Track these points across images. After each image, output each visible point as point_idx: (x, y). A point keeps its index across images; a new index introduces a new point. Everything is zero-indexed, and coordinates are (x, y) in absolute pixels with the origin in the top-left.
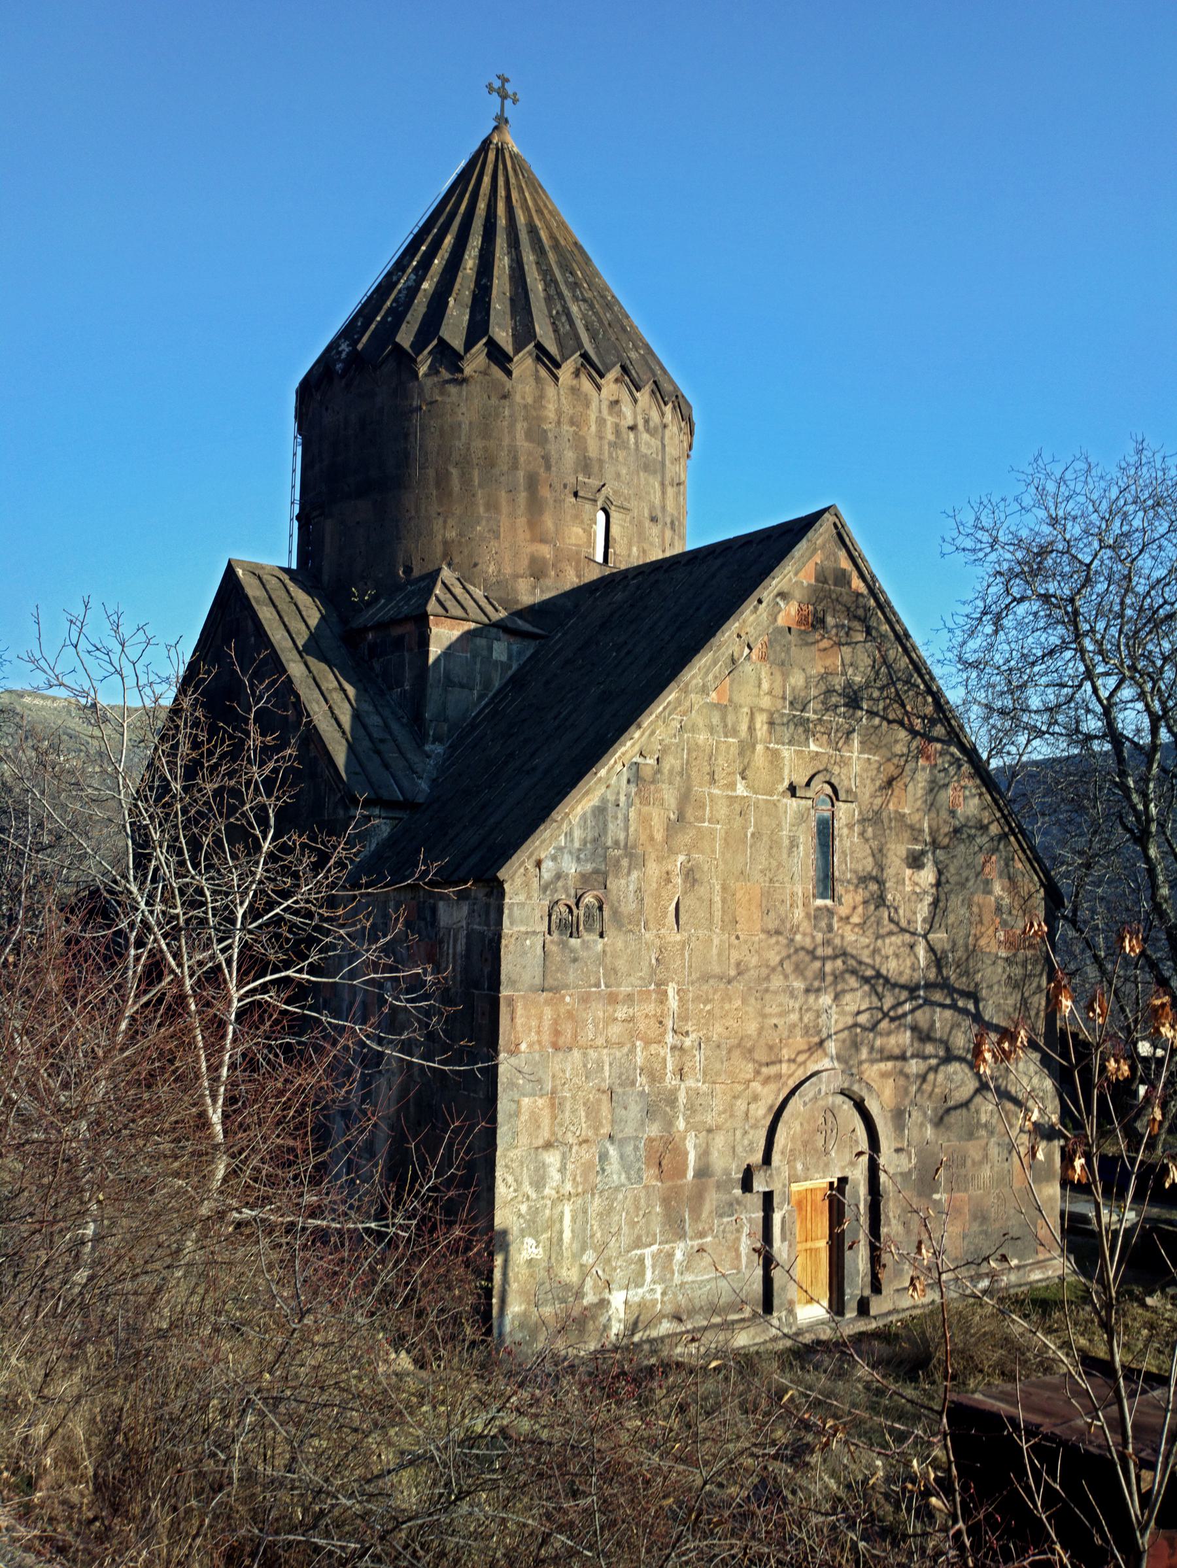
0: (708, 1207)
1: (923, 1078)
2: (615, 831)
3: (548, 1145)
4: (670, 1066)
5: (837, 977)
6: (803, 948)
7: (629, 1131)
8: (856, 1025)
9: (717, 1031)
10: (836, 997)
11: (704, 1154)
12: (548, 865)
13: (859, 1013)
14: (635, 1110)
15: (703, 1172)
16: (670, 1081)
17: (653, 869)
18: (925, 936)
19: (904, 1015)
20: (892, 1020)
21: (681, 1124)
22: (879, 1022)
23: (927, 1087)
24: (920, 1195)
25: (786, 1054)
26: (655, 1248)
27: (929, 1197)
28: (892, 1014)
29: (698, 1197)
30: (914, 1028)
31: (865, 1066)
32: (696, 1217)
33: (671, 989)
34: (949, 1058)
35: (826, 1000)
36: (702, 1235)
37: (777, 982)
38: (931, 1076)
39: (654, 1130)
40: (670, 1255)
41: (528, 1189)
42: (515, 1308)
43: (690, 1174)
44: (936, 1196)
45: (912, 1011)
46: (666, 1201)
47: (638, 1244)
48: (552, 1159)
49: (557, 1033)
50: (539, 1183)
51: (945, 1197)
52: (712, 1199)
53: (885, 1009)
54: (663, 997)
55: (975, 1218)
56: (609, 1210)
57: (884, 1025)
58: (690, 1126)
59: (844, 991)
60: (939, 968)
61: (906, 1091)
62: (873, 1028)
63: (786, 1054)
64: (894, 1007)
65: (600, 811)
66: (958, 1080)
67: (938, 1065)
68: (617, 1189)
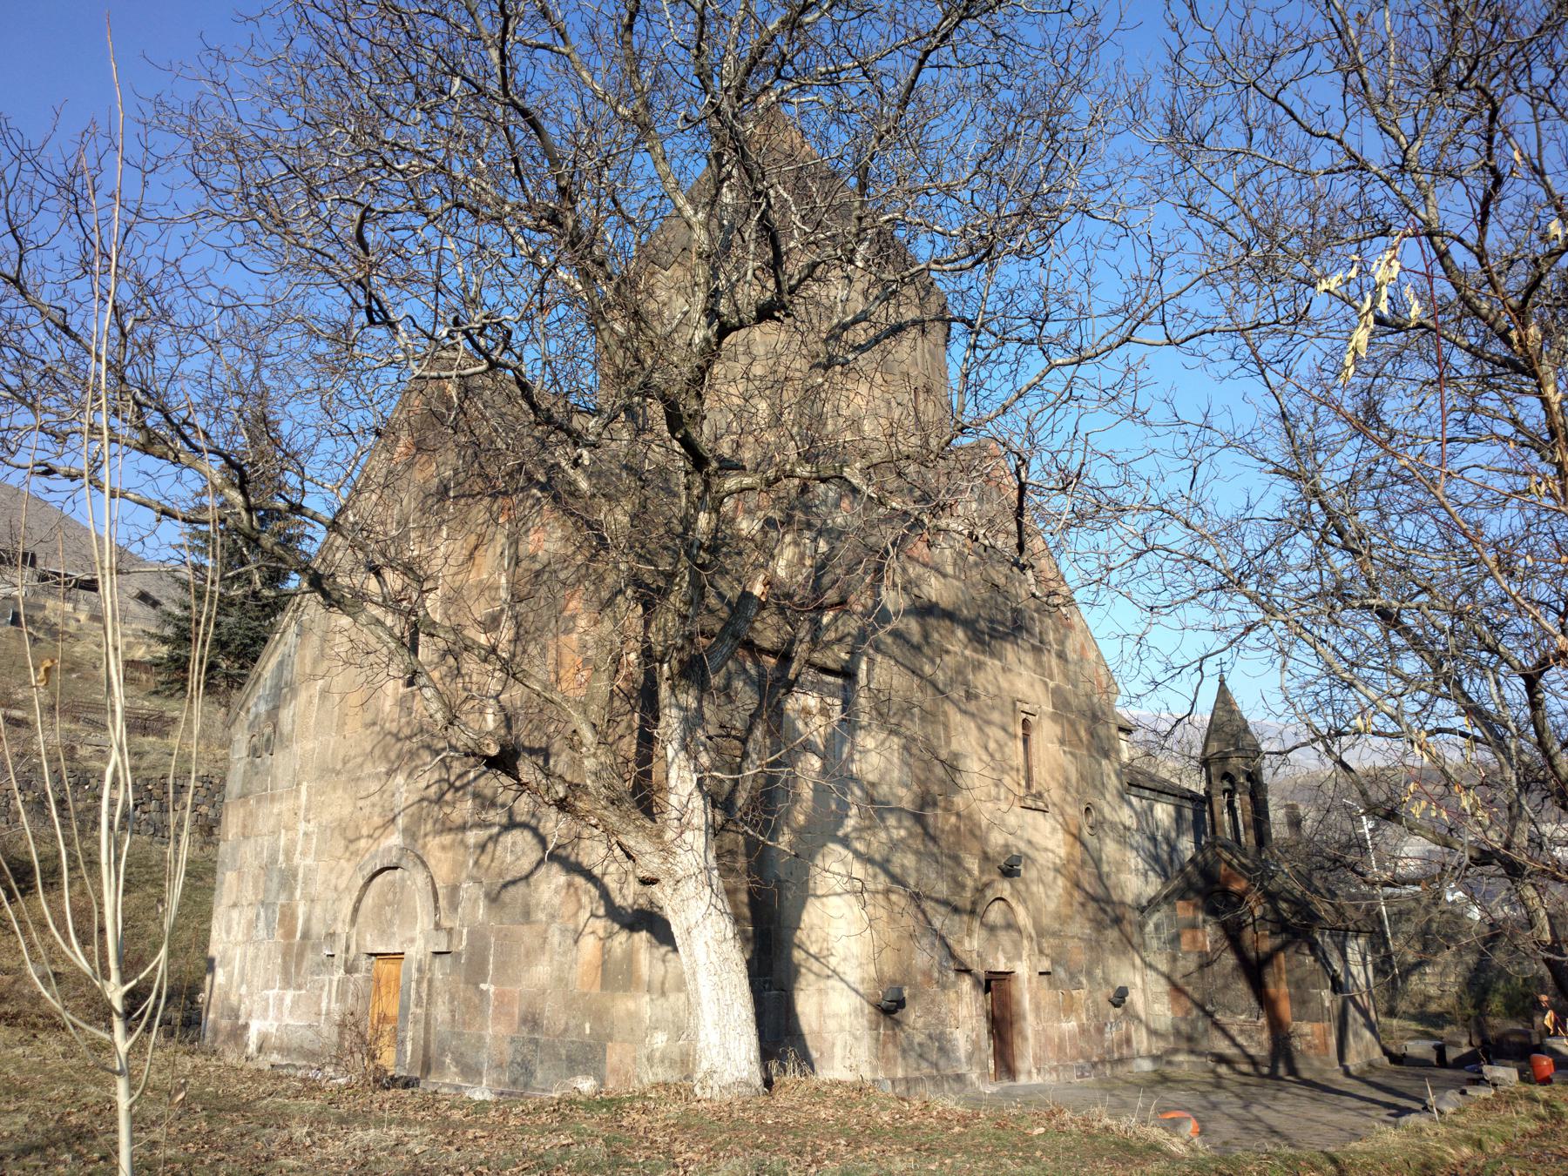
0: (306, 964)
1: (483, 847)
2: (287, 676)
3: (235, 905)
4: (299, 848)
5: (413, 754)
6: (390, 733)
7: (271, 899)
8: (422, 800)
9: (326, 817)
10: (410, 775)
11: (308, 920)
12: (253, 710)
13: (428, 787)
14: (274, 885)
15: (306, 935)
16: (297, 859)
17: (303, 696)
18: (496, 698)
19: (469, 783)
20: (457, 790)
21: (298, 894)
22: (443, 794)
23: (485, 860)
24: (467, 982)
25: (365, 831)
26: (276, 991)
27: (476, 985)
28: (458, 784)
29: (301, 955)
30: (476, 795)
31: (429, 838)
32: (298, 973)
33: (303, 788)
34: (511, 825)
35: (400, 779)
36: (299, 987)
37: (368, 768)
38: (490, 846)
39: (282, 900)
40: (282, 1000)
41: (224, 935)
42: (211, 1016)
43: (298, 935)
44: (483, 986)
45: (475, 779)
46: (284, 955)
47: (267, 986)
48: (235, 914)
49: (245, 826)
50: (228, 932)
51: (492, 989)
52: (310, 956)
53: (452, 778)
54: (298, 791)
55: (524, 1021)
56: (257, 956)
57: (448, 797)
58: (303, 896)
59: (416, 767)
60: (509, 727)
61: (464, 864)
62: (439, 800)
63: (365, 831)
64: (460, 776)
65: (281, 663)
66: (518, 850)
67: (499, 834)
68: (261, 941)
